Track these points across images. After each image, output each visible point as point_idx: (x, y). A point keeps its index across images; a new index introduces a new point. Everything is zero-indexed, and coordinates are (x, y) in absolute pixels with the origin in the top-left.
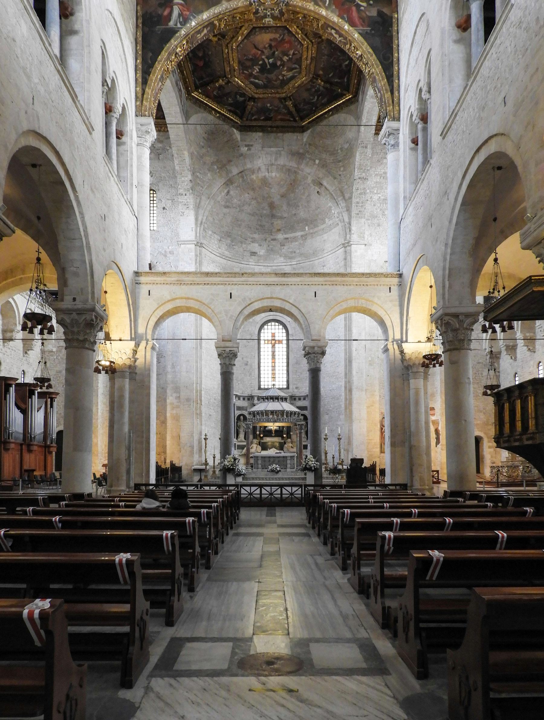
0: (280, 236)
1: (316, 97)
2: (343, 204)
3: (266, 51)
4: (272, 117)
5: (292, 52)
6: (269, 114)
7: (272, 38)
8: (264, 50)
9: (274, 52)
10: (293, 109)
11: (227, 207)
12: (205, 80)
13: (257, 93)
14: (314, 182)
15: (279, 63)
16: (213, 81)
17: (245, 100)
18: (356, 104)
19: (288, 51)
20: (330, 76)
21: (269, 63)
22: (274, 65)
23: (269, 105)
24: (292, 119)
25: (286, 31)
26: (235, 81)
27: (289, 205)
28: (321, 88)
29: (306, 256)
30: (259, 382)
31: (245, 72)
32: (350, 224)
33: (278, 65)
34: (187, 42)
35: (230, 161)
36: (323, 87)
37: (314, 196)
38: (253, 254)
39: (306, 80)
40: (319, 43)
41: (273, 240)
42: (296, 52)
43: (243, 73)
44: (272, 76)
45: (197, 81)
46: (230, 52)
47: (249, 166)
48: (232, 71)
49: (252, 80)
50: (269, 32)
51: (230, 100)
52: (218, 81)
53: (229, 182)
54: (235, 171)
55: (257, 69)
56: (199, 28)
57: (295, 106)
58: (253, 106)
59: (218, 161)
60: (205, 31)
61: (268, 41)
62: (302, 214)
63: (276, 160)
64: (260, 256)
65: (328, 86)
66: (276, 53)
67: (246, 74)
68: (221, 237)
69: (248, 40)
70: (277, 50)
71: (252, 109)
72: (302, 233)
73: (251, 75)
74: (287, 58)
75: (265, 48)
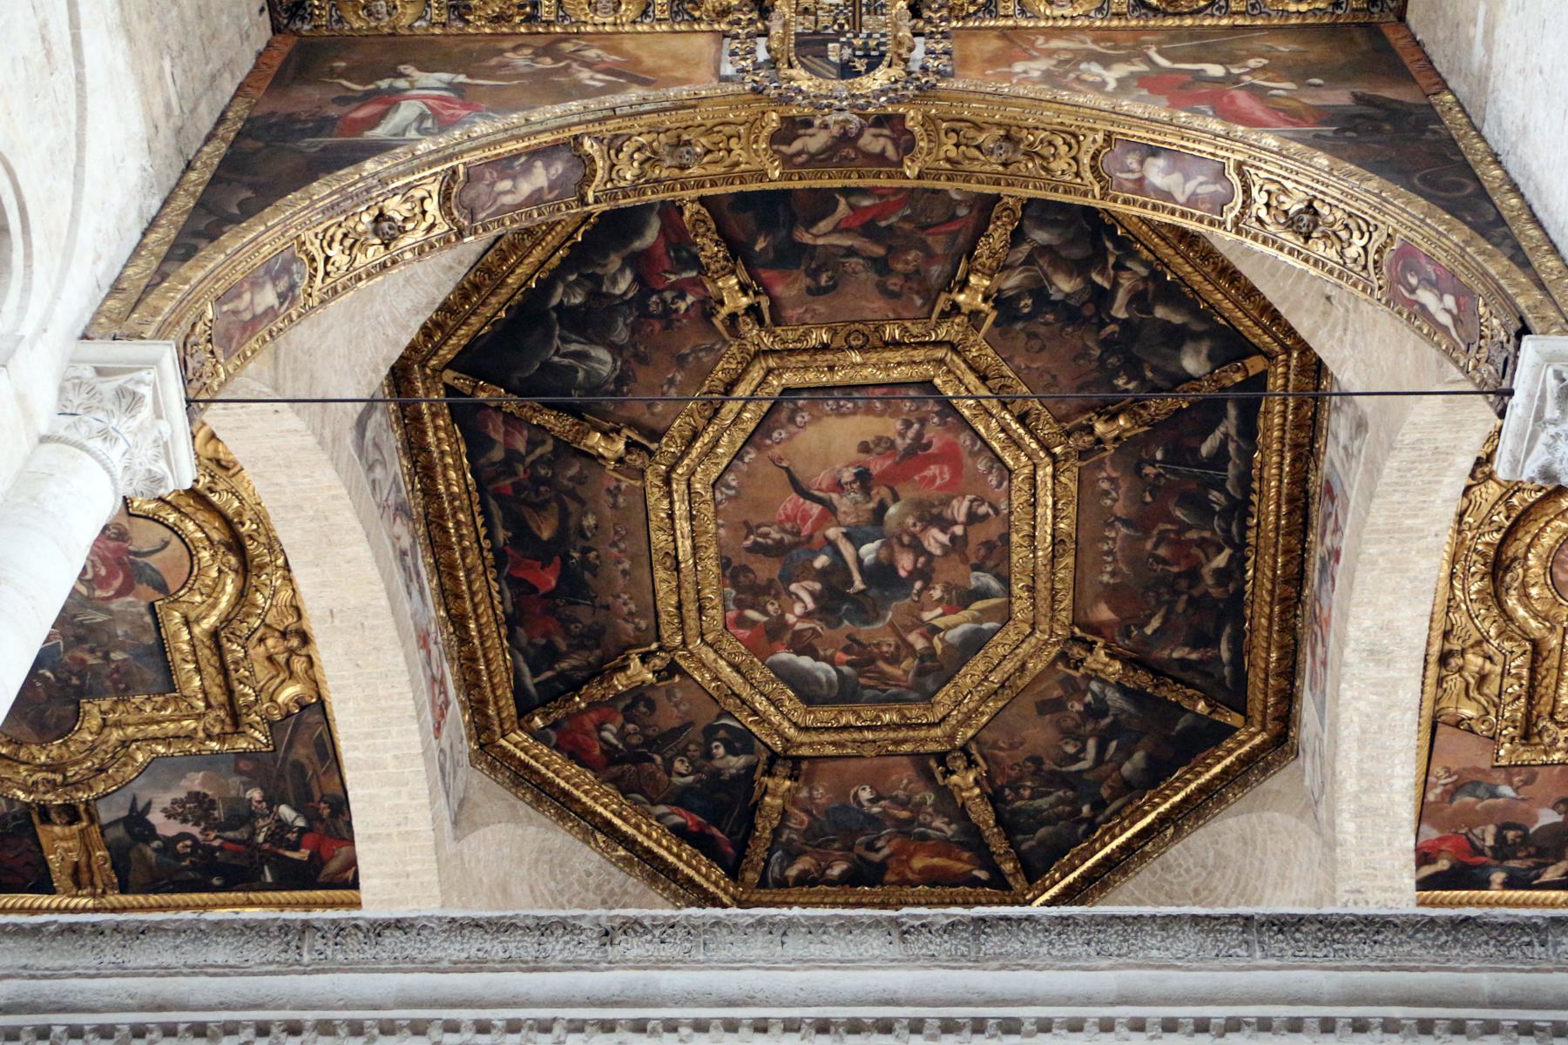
1: (1091, 744)
3: (843, 503)
4: (882, 867)
5: (966, 504)
6: (871, 847)
7: (869, 439)
8: (835, 496)
9: (882, 508)
10: (983, 814)
12: (564, 665)
13: (807, 729)
15: (905, 563)
16: (599, 672)
17: (751, 769)
18: (1291, 767)
19: (946, 503)
20: (1149, 631)
21: (859, 561)
22: (882, 575)
23: (865, 795)
24: (982, 875)
25: (932, 406)
26: (703, 665)
28: (1112, 696)
31: (752, 614)
33: (903, 573)
34: (445, 196)
36: (1119, 686)
39: (1038, 650)
40: (1083, 454)
42: (983, 509)
43: (741, 621)
44: (877, 633)
45: (526, 670)
46: (681, 509)
48: (691, 609)
49: (784, 656)
50: (854, 413)
51: (683, 773)
52: (624, 668)
55: (804, 593)
56: (513, 146)
57: (994, 798)
58: (791, 798)
60: (540, 177)
61: (853, 453)
65: (1143, 679)
66: (893, 510)
67: (754, 623)
69: (759, 448)
70: (896, 499)
71: (784, 814)
73: (776, 631)
74: (944, 539)
75: (838, 486)
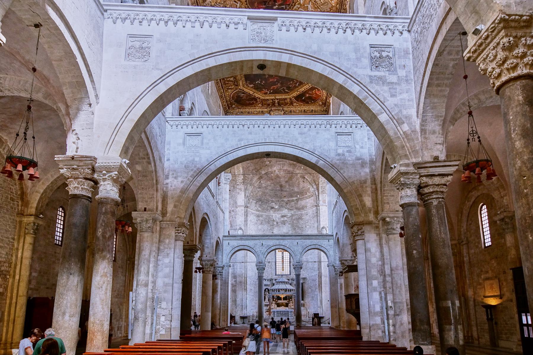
0: (286, 199)
2: (315, 187)
11: (260, 188)
14: (301, 176)
27: (289, 185)
29: (298, 209)
30: (276, 271)
32: (319, 196)
35: (261, 168)
37: (301, 183)
38: (272, 208)
41: (283, 201)
47: (270, 170)
53: (261, 178)
54: (263, 172)
59: (255, 169)
62: (296, 189)
63: (283, 167)
64: (275, 209)
68: (257, 201)
72: (296, 198)
